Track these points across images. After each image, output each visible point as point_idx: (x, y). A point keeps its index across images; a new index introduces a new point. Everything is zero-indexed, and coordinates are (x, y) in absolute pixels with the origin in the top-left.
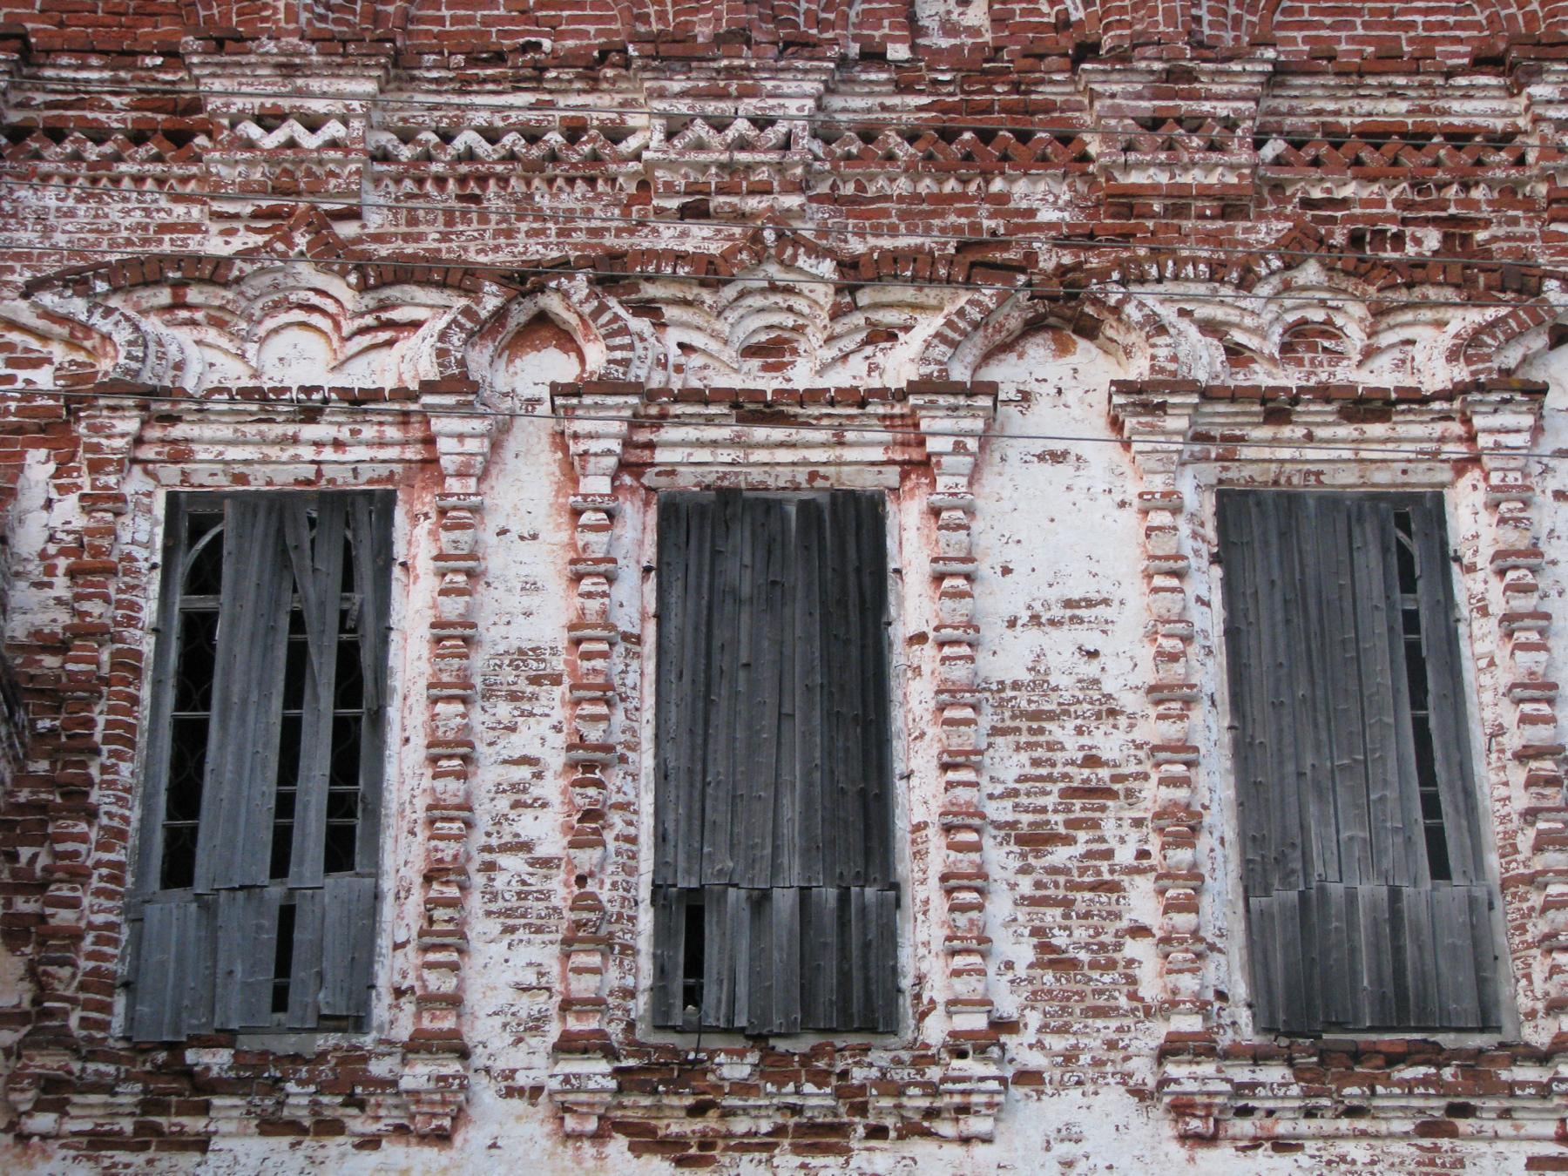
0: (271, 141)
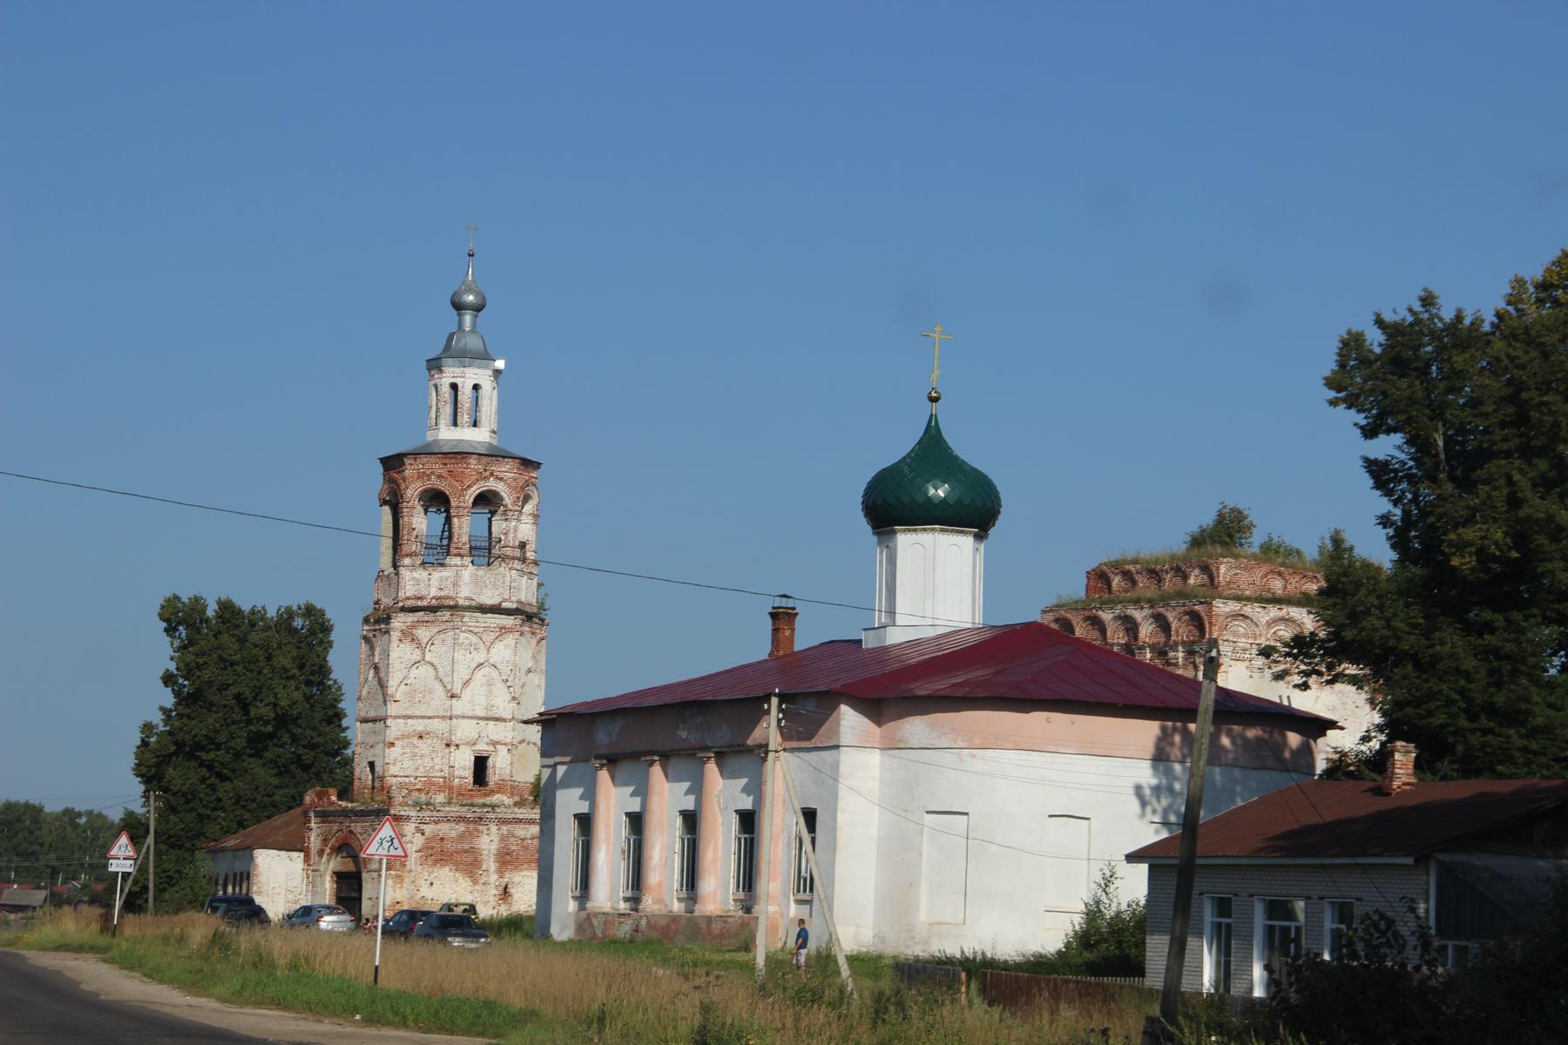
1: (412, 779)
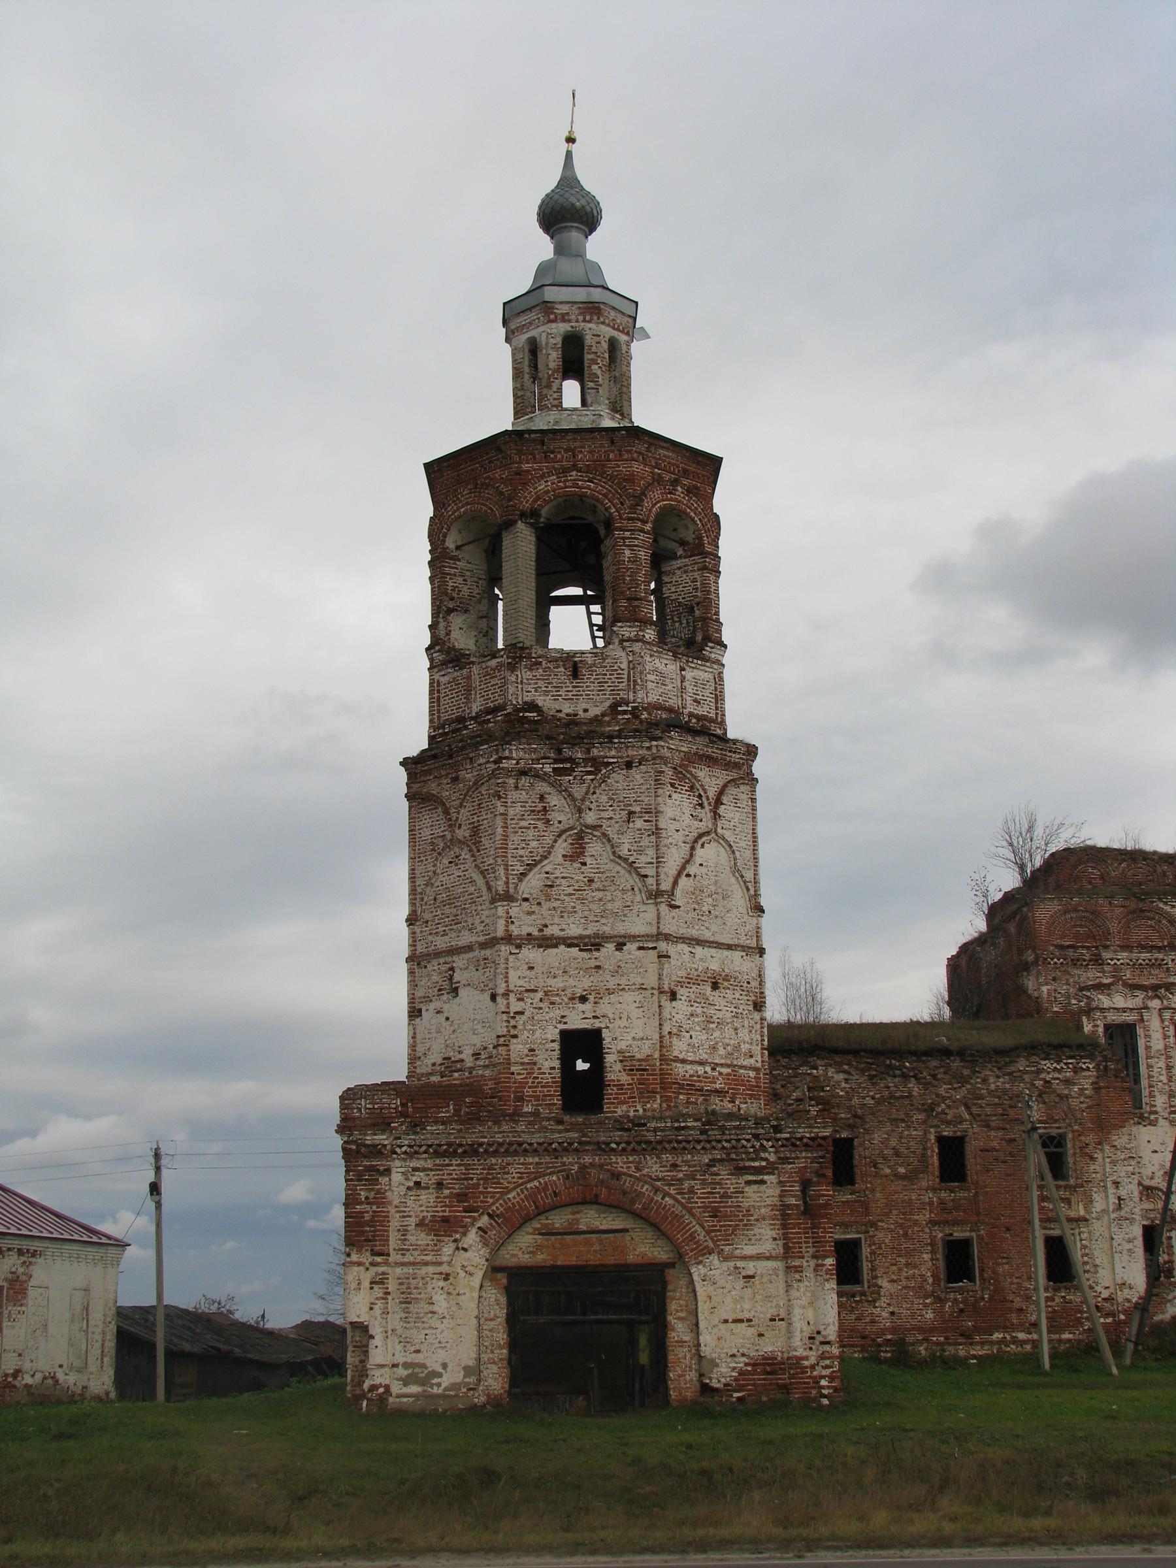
0: (1112, 963)
1: (708, 1069)
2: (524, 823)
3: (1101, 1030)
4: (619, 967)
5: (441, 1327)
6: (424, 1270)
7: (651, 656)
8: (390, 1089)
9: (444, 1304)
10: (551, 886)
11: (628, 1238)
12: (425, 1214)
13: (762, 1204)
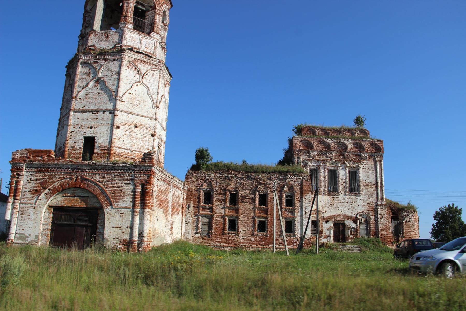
1: (130, 151)
2: (83, 77)
3: (309, 170)
4: (103, 118)
5: (31, 223)
6: (28, 205)
7: (130, 33)
8: (27, 151)
9: (32, 216)
10: (88, 95)
11: (89, 199)
12: (31, 188)
13: (129, 191)
